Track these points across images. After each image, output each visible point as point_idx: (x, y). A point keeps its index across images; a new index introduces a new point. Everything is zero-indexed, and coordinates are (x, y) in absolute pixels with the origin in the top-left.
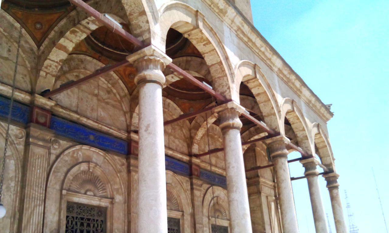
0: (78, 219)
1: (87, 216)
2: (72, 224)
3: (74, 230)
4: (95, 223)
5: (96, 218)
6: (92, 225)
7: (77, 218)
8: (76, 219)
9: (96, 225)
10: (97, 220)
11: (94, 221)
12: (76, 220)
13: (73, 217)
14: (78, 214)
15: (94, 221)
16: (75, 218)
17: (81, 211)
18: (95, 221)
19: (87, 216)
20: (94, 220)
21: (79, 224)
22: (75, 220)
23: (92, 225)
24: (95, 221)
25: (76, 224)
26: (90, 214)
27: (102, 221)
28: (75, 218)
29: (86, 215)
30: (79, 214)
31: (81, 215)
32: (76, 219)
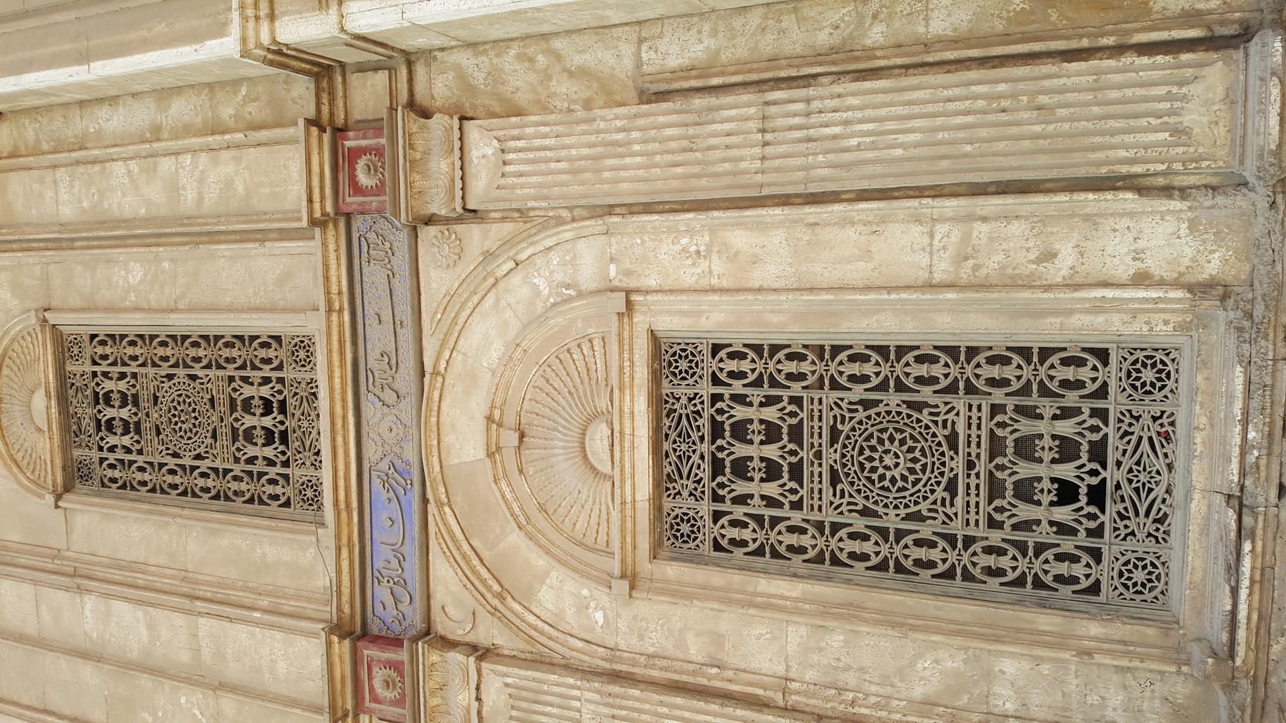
0: (1095, 421)
1: (1118, 487)
3: (1034, 400)
5: (1110, 546)
7: (1102, 414)
8: (1095, 413)
9: (1068, 545)
10: (1096, 554)
12: (1087, 412)
13: (1102, 392)
14: (1125, 427)
15: (1091, 533)
16: (1100, 404)
17: (1145, 445)
19: (1118, 487)
20: (1097, 532)
21: (1066, 428)
22: (1086, 408)
25: (1066, 413)
26: (1128, 504)
27: (1095, 589)
28: (1100, 404)
29: (1120, 475)
30: (1126, 433)
31: (1121, 448)
32: (1095, 413)
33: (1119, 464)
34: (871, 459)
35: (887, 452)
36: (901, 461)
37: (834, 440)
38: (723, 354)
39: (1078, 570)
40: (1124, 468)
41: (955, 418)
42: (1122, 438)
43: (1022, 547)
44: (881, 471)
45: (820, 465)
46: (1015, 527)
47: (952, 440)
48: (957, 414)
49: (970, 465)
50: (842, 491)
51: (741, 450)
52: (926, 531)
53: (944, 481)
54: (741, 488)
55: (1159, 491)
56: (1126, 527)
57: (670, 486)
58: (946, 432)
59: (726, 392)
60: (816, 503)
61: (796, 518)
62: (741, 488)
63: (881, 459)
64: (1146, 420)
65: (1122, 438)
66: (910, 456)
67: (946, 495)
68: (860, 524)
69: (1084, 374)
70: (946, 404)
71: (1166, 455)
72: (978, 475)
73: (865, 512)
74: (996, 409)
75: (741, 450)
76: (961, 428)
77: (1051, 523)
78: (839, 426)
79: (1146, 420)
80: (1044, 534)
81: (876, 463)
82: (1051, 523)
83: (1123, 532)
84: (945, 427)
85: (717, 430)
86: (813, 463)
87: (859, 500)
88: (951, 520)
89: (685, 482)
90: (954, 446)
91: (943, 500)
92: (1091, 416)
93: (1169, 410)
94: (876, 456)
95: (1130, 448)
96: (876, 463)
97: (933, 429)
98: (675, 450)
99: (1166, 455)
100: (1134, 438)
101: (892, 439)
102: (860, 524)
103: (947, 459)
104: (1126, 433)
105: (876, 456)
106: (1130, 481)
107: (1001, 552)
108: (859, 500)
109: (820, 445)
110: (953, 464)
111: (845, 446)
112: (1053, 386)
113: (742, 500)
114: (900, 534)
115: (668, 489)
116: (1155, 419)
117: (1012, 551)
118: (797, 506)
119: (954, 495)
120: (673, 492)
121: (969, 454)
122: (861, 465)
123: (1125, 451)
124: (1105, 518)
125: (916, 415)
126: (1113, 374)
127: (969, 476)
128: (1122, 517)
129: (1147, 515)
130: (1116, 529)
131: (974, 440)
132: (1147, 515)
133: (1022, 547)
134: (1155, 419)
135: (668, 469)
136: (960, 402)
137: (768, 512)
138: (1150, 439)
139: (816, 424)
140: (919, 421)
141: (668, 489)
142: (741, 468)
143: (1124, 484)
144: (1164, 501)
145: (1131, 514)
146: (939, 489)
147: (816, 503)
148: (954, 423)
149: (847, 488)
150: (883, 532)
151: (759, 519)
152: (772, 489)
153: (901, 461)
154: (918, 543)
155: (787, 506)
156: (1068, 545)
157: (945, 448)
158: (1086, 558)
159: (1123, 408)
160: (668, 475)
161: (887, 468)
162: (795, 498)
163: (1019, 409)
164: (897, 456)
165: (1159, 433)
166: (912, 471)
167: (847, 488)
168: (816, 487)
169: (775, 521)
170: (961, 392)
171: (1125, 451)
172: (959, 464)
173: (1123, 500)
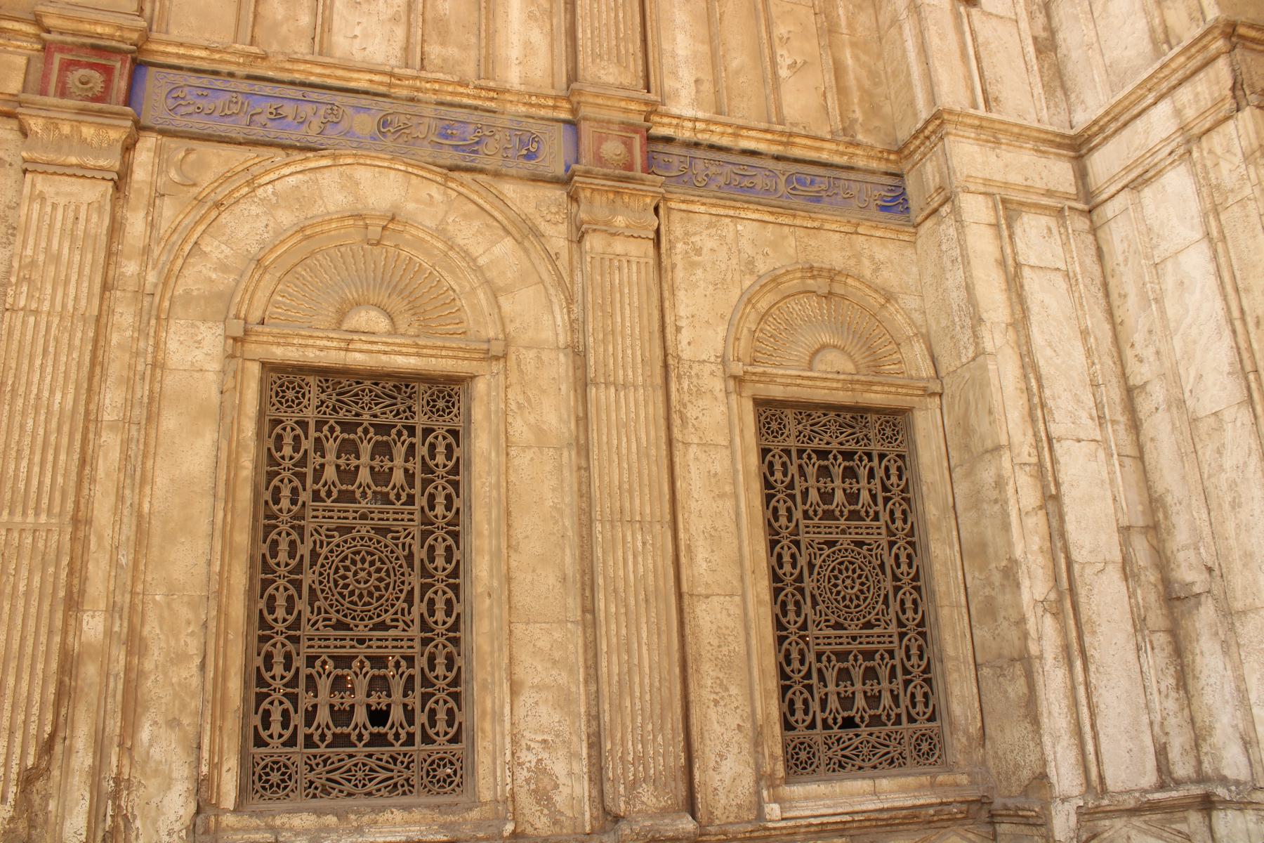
0: (403, 736)
1: (351, 756)
2: (433, 712)
4: (302, 731)
5: (298, 754)
6: (323, 716)
9: (297, 719)
10: (291, 742)
11: (308, 738)
13: (427, 739)
14: (401, 758)
15: (308, 738)
18: (301, 739)
23: (323, 716)
24: (301, 739)
25: (409, 715)
26: (337, 765)
28: (418, 738)
29: (360, 758)
31: (385, 757)
33: (370, 756)
34: (363, 560)
35: (370, 574)
36: (362, 585)
37: (378, 530)
38: (451, 439)
39: (276, 728)
40: (367, 760)
41: (400, 628)
42: (391, 757)
43: (294, 683)
44: (353, 568)
45: (355, 518)
46: (310, 677)
47: (382, 626)
48: (404, 630)
49: (361, 641)
50: (333, 537)
51: (366, 448)
52: (301, 605)
53: (348, 620)
54: (331, 446)
55: (348, 787)
56: (317, 765)
57: (330, 383)
58: (388, 622)
59: (417, 440)
60: (320, 514)
61: (305, 496)
62: (331, 446)
63: (363, 570)
64: (406, 774)
65: (391, 757)
66: (365, 593)
67: (334, 620)
68: (304, 550)
69: (441, 726)
70: (412, 621)
71: (379, 790)
72: (353, 647)
73: (314, 555)
74: (410, 660)
75: (366, 448)
76: (392, 632)
77: (315, 706)
78: (390, 536)
79: (406, 774)
80: (306, 700)
81: (359, 565)
82: (315, 706)
83: (313, 762)
84: (393, 620)
85: (383, 429)
86: (356, 512)
87: (325, 551)
88: (313, 626)
89: (334, 397)
90: (377, 627)
91: (330, 620)
92: (408, 733)
93: (415, 791)
94: (366, 565)
95: (383, 764)
96: (359, 565)
97: (392, 611)
98: (363, 391)
99: (379, 790)
100: (392, 766)
101: (380, 580)
102: (304, 550)
103: (366, 622)
104: (395, 760)
105: (366, 565)
106: (356, 765)
107: (287, 667)
108: (325, 551)
109: (372, 519)
110: (361, 627)
111: (371, 539)
112: (430, 704)
113: (319, 446)
114: (298, 585)
115: (327, 381)
116: (407, 780)
117: (289, 675)
118: (316, 496)
119: (334, 627)
120: (325, 385)
121: (370, 640)
122: (358, 553)
123: (381, 760)
124: (322, 749)
125: (403, 596)
126: (441, 747)
127: (352, 640)
128: (325, 761)
129: (328, 779)
130: (315, 757)
131: (384, 643)
132: (328, 779)
133: (294, 683)
134: (407, 780)
135: (345, 383)
136: (415, 631)
137: (309, 471)
138: (392, 778)
139: (391, 516)
140: (398, 599)
141: (327, 381)
142: (349, 448)
143: (354, 760)
144: (341, 791)
145: (328, 768)
146: (340, 616)
147: (320, 514)
148: (396, 627)
149: (336, 540)
150: (299, 569)
151: (303, 462)
152: (330, 473)
153: (362, 585)
154: (290, 599)
155: (316, 487)
156: (297, 719)
157: (376, 620)
158: (287, 734)
159: (415, 757)
160: (340, 383)
161: (355, 574)
162: (323, 494)
163: (411, 677)
164: (366, 582)
165: (395, 785)
166: (352, 593)
167: (336, 540)
168: (335, 514)
169: (302, 477)
170: (423, 635)
171: (381, 760)
172: (361, 631)
173: (340, 761)
